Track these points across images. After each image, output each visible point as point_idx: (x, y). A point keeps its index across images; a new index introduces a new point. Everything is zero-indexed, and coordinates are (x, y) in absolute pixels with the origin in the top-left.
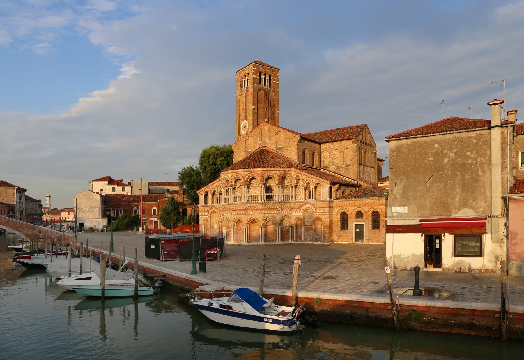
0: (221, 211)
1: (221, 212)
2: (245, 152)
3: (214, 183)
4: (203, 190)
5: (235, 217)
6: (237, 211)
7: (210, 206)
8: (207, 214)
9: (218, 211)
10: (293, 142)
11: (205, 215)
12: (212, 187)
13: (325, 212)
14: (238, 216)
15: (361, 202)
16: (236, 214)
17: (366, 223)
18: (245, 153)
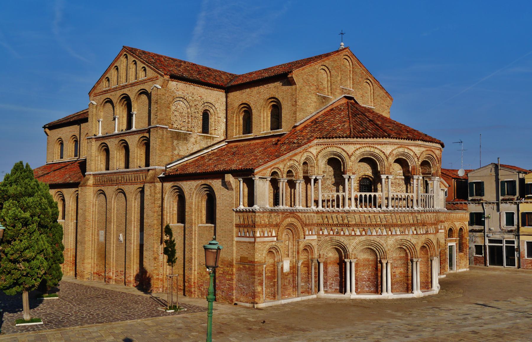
0: (306, 225)
1: (306, 229)
2: (318, 96)
3: (296, 154)
4: (268, 168)
5: (423, 238)
6: (426, 227)
7: (284, 212)
8: (274, 234)
9: (299, 225)
10: (385, 106)
11: (268, 237)
12: (292, 162)
13: (441, 228)
14: (427, 236)
15: (454, 215)
16: (424, 233)
17: (456, 244)
18: (317, 97)
